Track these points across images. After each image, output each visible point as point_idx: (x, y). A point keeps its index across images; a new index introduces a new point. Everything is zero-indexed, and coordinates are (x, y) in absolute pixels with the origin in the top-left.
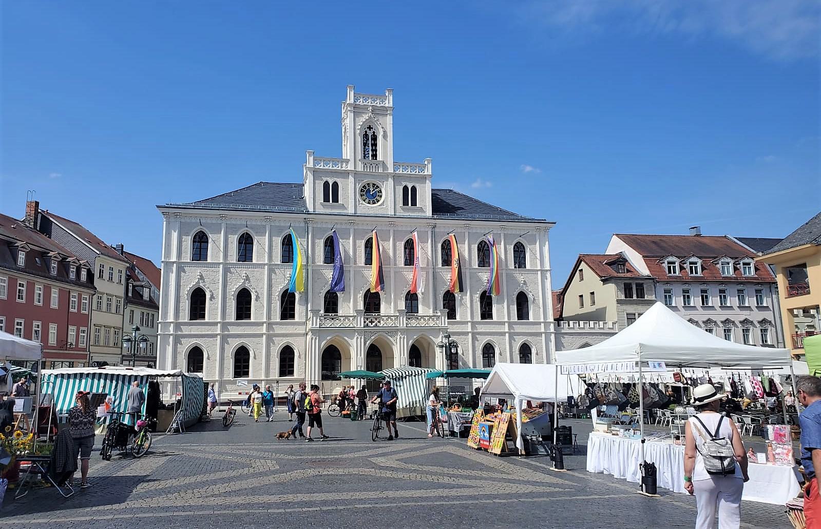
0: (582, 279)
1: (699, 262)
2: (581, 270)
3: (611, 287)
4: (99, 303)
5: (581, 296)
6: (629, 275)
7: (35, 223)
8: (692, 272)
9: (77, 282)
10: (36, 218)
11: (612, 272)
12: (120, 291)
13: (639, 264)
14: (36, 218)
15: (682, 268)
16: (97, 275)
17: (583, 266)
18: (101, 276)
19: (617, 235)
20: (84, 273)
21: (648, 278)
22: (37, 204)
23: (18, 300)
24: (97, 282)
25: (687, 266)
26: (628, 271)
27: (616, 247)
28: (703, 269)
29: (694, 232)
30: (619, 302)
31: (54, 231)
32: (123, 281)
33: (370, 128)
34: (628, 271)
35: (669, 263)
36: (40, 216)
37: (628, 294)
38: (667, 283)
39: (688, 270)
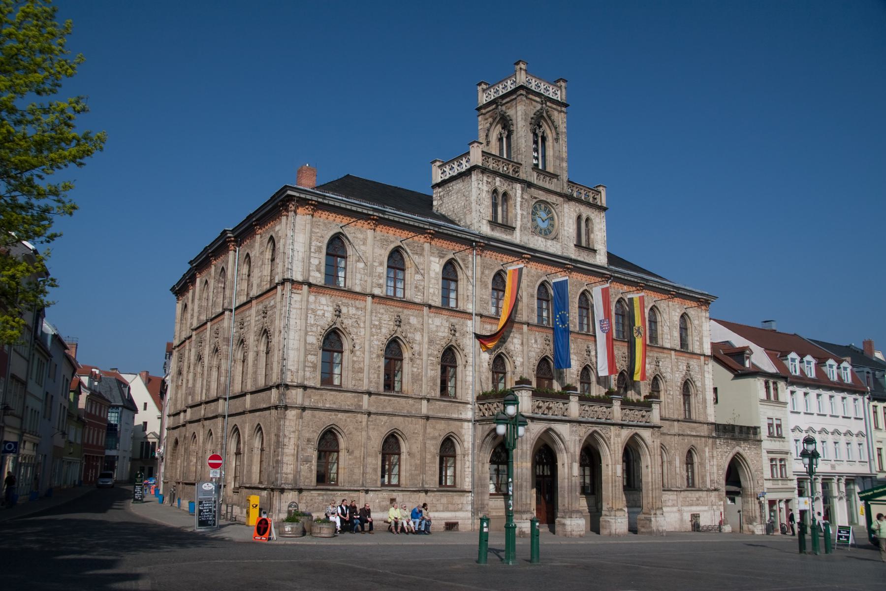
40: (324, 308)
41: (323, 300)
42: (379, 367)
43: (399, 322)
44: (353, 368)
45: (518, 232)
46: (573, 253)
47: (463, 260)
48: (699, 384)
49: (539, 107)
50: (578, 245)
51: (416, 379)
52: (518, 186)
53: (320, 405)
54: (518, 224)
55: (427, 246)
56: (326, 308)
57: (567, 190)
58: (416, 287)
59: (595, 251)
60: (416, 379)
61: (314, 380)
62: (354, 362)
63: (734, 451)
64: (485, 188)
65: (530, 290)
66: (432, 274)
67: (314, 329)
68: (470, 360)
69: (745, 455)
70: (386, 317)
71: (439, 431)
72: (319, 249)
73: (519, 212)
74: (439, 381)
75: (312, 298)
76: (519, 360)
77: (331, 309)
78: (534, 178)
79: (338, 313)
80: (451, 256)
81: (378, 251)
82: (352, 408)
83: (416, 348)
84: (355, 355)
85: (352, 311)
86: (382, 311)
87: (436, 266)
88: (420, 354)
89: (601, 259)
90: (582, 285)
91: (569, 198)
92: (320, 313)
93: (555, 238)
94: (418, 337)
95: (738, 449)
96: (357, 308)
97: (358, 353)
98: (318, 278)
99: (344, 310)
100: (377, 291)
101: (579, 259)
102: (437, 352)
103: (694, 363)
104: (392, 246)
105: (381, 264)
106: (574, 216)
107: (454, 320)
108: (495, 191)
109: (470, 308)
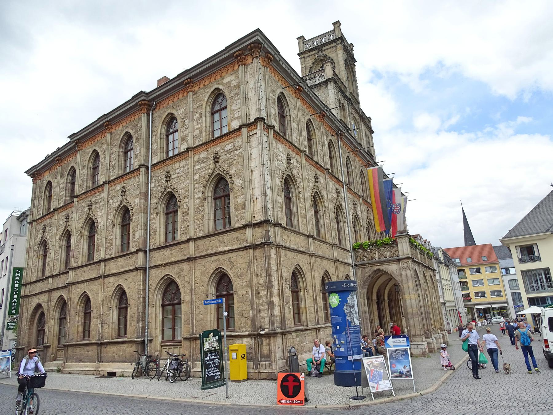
42: (312, 215)
44: (301, 213)
53: (288, 245)
56: (282, 155)
58: (320, 155)
62: (301, 208)
67: (278, 172)
70: (310, 173)
77: (285, 157)
82: (304, 250)
84: (300, 202)
85: (295, 163)
86: (308, 168)
92: (280, 158)
96: (297, 161)
97: (302, 200)
104: (308, 117)
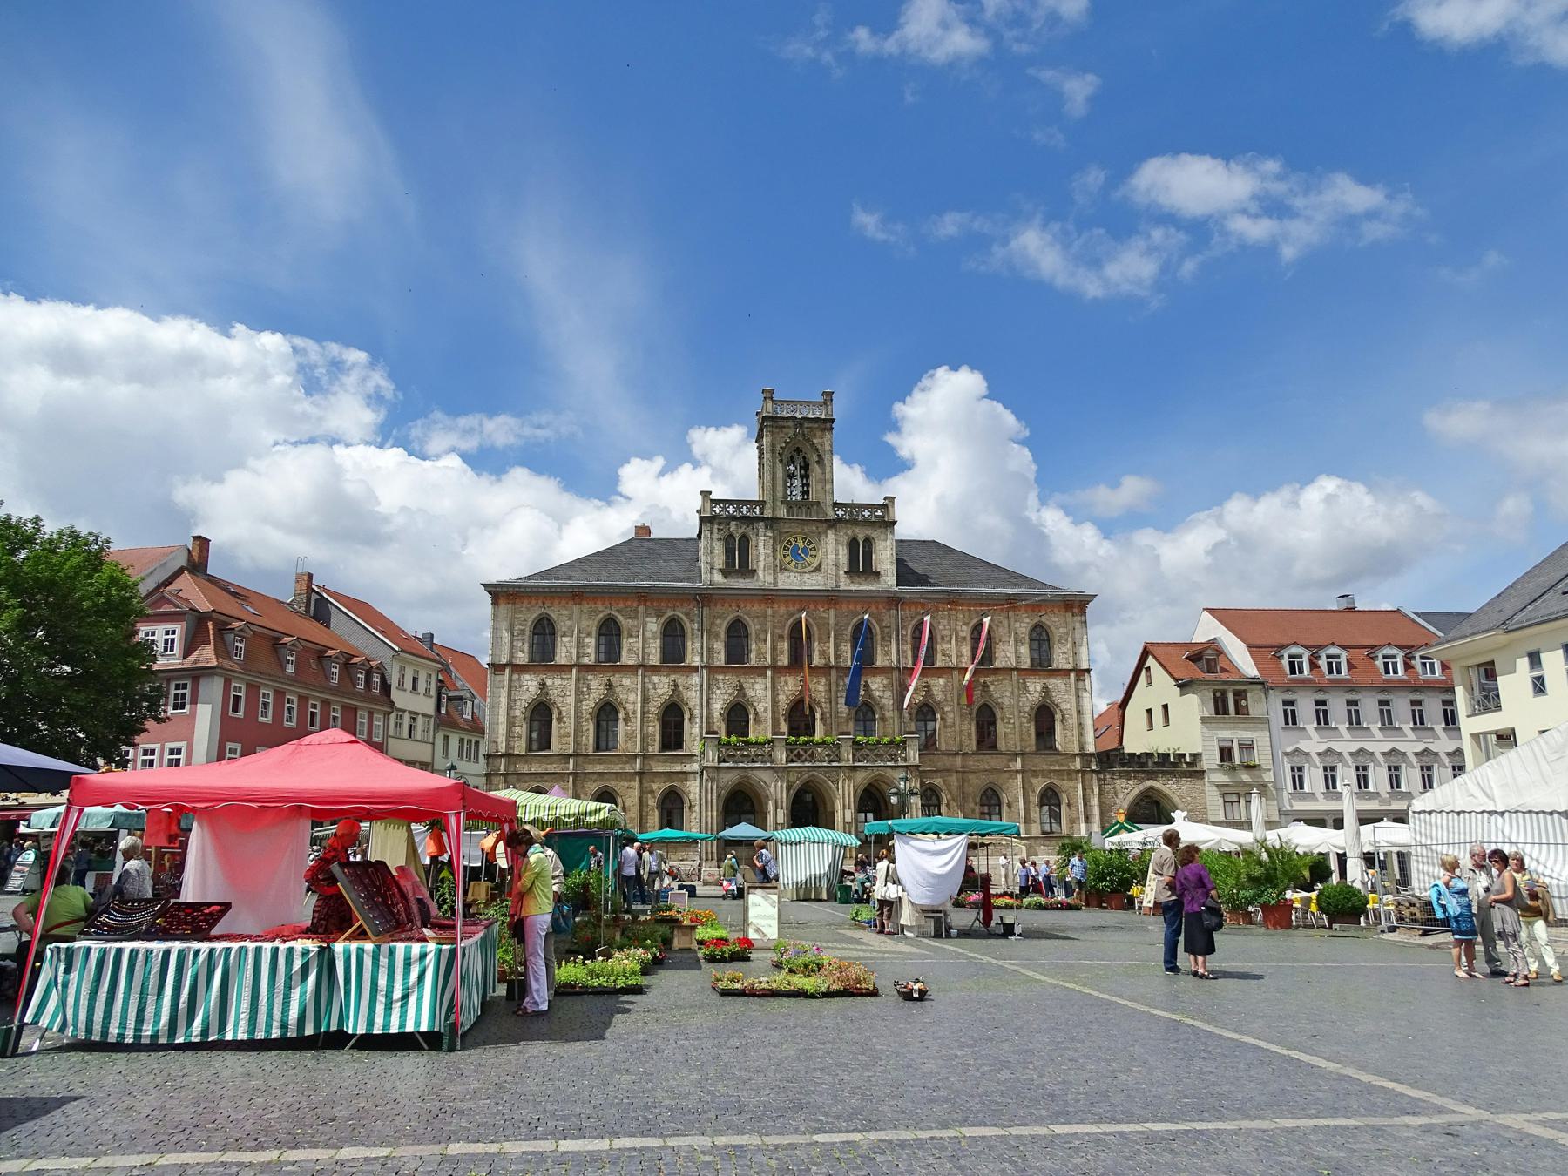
0: (1149, 684)
1: (1344, 655)
2: (1148, 669)
3: (1193, 699)
4: (398, 725)
5: (1149, 711)
6: (1224, 676)
7: (308, 606)
8: (1331, 672)
9: (367, 696)
10: (309, 598)
11: (1194, 671)
12: (428, 706)
13: (1244, 662)
14: (309, 598)
15: (1314, 666)
16: (394, 683)
17: (1151, 662)
18: (401, 684)
19: (1210, 610)
20: (377, 679)
21: (1253, 682)
22: (310, 576)
23: (286, 724)
24: (396, 695)
25: (1323, 663)
26: (1223, 670)
27: (1208, 630)
28: (1350, 666)
29: (1344, 604)
30: (1203, 720)
31: (335, 619)
32: (433, 692)
33: (798, 451)
34: (1223, 670)
35: (1291, 657)
36: (314, 597)
37: (1220, 707)
38: (1288, 690)
39: (1324, 668)
40: (530, 685)
41: (527, 677)
43: (610, 685)
45: (760, 573)
46: (845, 584)
47: (687, 615)
48: (1064, 706)
49: (791, 432)
50: (852, 571)
51: (630, 736)
52: (761, 524)
54: (761, 564)
55: (641, 609)
57: (831, 515)
59: (878, 574)
60: (630, 736)
61: (520, 748)
63: (1142, 787)
64: (716, 536)
65: (778, 631)
66: (648, 634)
68: (697, 712)
69: (1167, 791)
71: (659, 787)
72: (522, 632)
73: (761, 550)
74: (658, 737)
75: (515, 677)
76: (761, 707)
78: (782, 513)
79: (543, 685)
80: (670, 613)
81: (584, 623)
83: (630, 707)
85: (558, 681)
87: (654, 626)
88: (634, 712)
89: (889, 580)
90: (856, 614)
91: (834, 524)
93: (818, 569)
94: (632, 697)
95: (1149, 783)
98: (522, 658)
99: (549, 682)
100: (586, 660)
101: (853, 587)
102: (654, 707)
103: (1056, 684)
105: (589, 635)
106: (845, 539)
107: (673, 677)
108: (731, 536)
109: (696, 661)
